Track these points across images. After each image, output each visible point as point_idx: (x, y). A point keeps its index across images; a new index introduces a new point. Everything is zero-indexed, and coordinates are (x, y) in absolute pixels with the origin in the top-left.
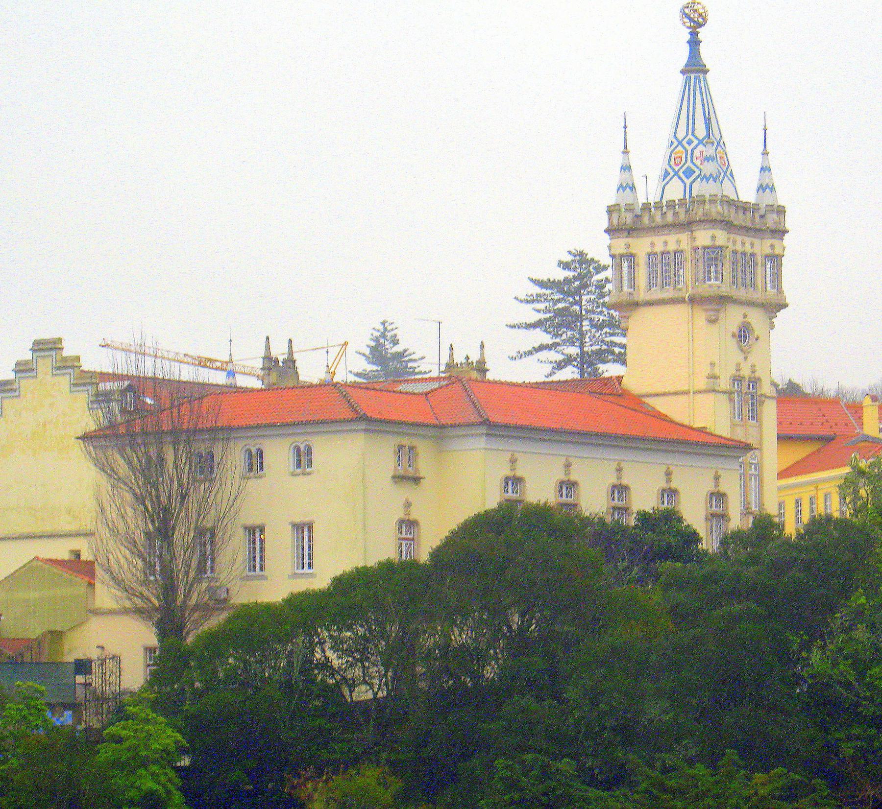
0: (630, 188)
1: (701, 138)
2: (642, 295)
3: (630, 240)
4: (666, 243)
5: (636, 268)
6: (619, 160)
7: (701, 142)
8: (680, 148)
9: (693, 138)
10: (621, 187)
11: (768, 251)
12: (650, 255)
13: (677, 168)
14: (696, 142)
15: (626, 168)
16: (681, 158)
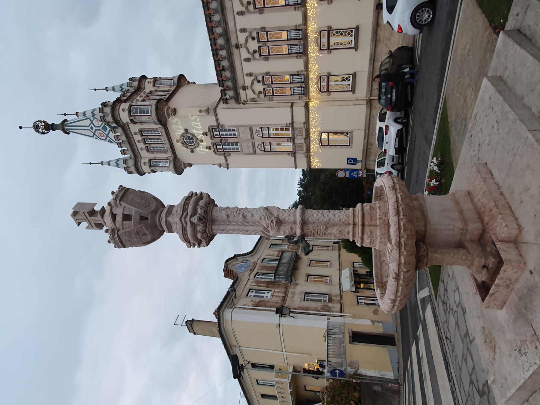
0: (117, 162)
1: (90, 122)
2: (169, 155)
3: (143, 161)
4: (139, 142)
5: (157, 158)
6: (106, 166)
7: (92, 122)
8: (96, 134)
9: (90, 127)
10: (117, 165)
11: (151, 84)
12: (148, 151)
13: (105, 136)
14: (92, 125)
15: (109, 163)
16: (100, 133)
